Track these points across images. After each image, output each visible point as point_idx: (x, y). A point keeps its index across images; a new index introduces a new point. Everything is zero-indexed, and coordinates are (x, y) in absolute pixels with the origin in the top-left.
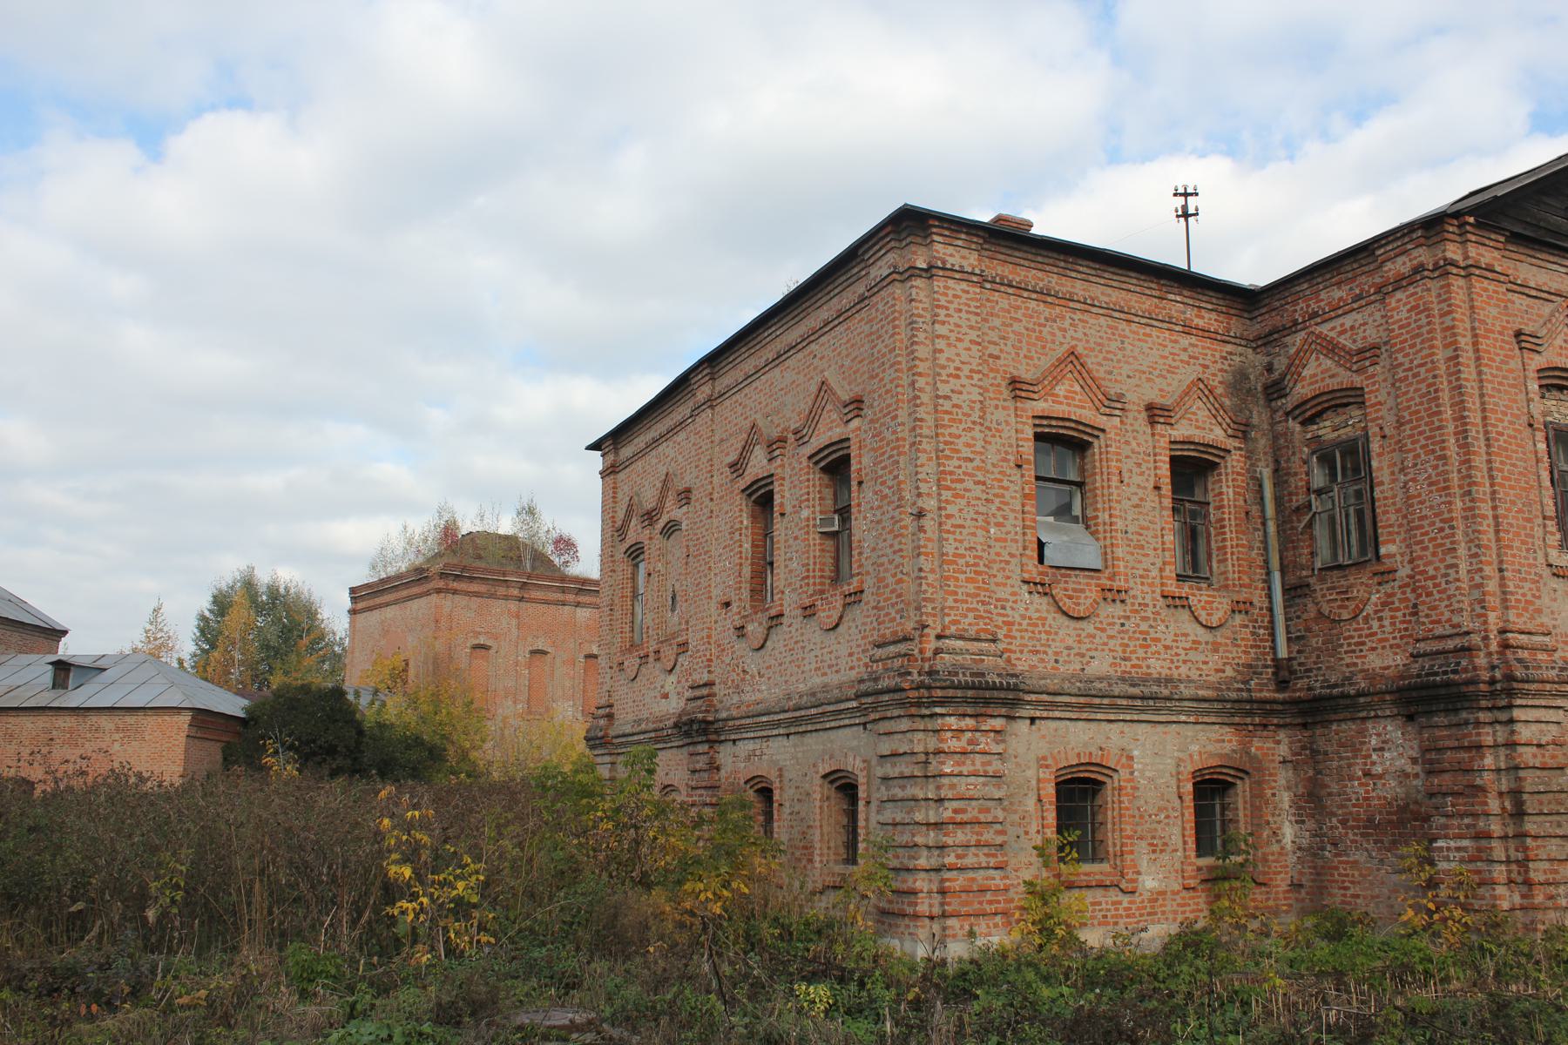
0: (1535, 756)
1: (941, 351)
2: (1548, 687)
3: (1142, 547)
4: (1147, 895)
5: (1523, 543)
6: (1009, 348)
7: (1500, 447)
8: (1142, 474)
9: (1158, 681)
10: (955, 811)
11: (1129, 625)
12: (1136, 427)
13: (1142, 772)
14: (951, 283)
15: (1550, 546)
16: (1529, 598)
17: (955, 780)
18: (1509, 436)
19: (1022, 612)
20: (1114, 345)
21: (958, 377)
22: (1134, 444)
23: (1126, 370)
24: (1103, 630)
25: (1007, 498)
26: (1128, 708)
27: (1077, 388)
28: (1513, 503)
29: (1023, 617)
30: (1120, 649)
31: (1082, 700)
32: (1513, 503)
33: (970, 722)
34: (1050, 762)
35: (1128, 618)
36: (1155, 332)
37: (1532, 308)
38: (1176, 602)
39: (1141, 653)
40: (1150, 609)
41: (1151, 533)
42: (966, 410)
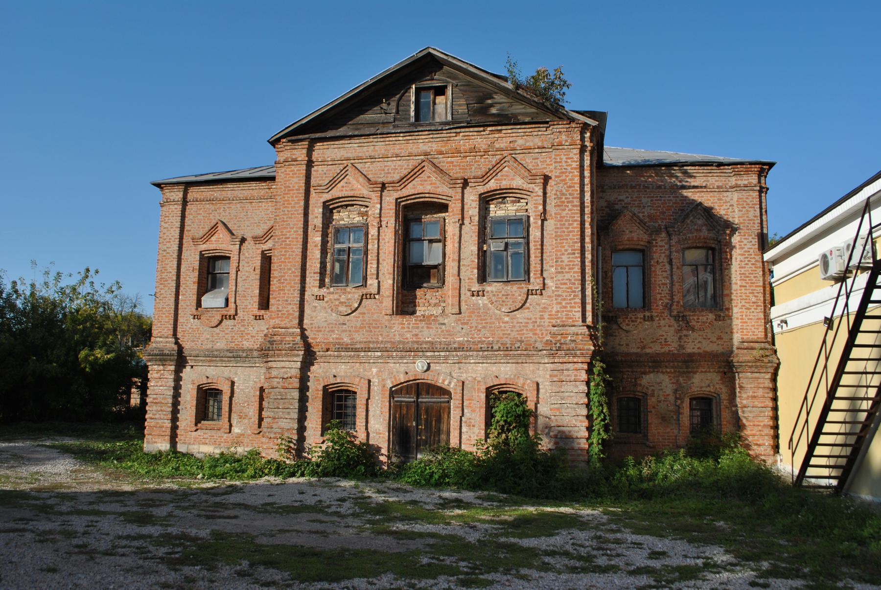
0: (278, 383)
1: (164, 234)
2: (284, 352)
3: (245, 296)
4: (235, 435)
5: (291, 287)
6: (195, 226)
7: (285, 245)
8: (249, 266)
9: (243, 351)
10: (154, 399)
11: (236, 329)
12: (249, 247)
13: (238, 386)
14: (171, 206)
15: (313, 286)
16: (291, 312)
17: (155, 388)
18: (292, 238)
19: (189, 326)
20: (242, 215)
21: (170, 242)
22: (247, 254)
23: (247, 223)
24: (223, 331)
25: (188, 284)
26: (228, 361)
27: (221, 236)
28: (290, 269)
29: (190, 328)
30: (230, 338)
31: (208, 358)
32: (290, 269)
33: (161, 367)
34: (195, 382)
35: (235, 326)
36: (264, 205)
37: (330, 170)
38: (257, 318)
39: (240, 339)
40: (247, 321)
41: (250, 290)
42: (171, 254)
